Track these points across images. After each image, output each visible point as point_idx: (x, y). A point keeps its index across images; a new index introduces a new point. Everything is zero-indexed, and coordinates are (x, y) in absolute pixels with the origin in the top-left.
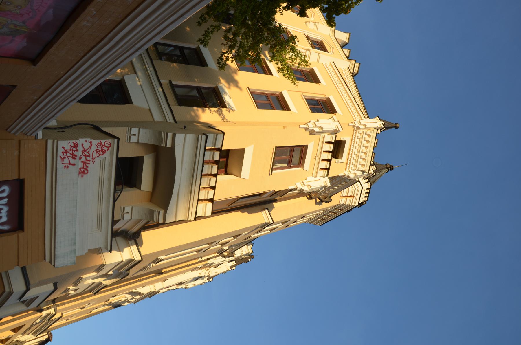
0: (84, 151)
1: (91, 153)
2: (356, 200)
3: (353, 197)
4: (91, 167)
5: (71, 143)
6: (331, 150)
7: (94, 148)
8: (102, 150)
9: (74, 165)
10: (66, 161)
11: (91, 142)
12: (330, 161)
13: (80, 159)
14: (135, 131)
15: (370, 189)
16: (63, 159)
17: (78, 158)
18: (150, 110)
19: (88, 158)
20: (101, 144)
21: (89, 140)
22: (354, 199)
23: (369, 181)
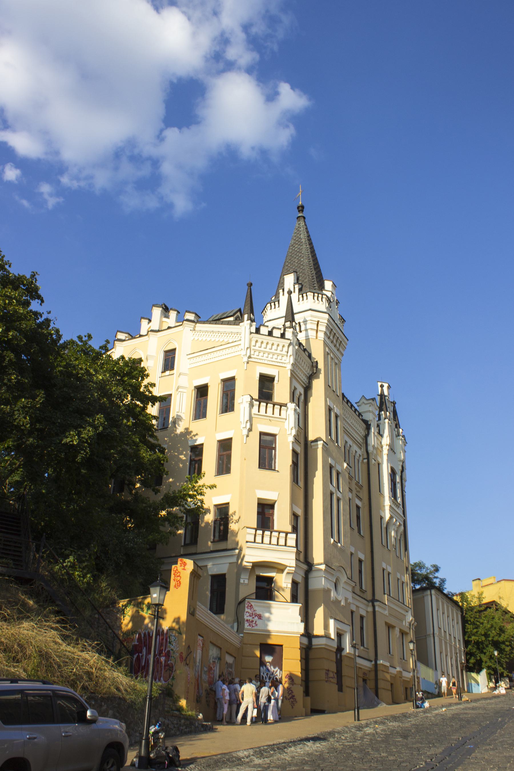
0: (250, 616)
1: (251, 612)
2: (322, 318)
3: (318, 322)
4: (258, 613)
5: (246, 622)
6: (265, 404)
7: (249, 611)
8: (251, 606)
9: (256, 622)
10: (254, 625)
11: (246, 612)
12: (274, 405)
13: (253, 618)
14: (242, 581)
15: (314, 293)
16: (253, 626)
17: (253, 620)
18: (230, 563)
19: (254, 614)
20: (247, 607)
21: (245, 614)
22: (321, 320)
23: (306, 293)
